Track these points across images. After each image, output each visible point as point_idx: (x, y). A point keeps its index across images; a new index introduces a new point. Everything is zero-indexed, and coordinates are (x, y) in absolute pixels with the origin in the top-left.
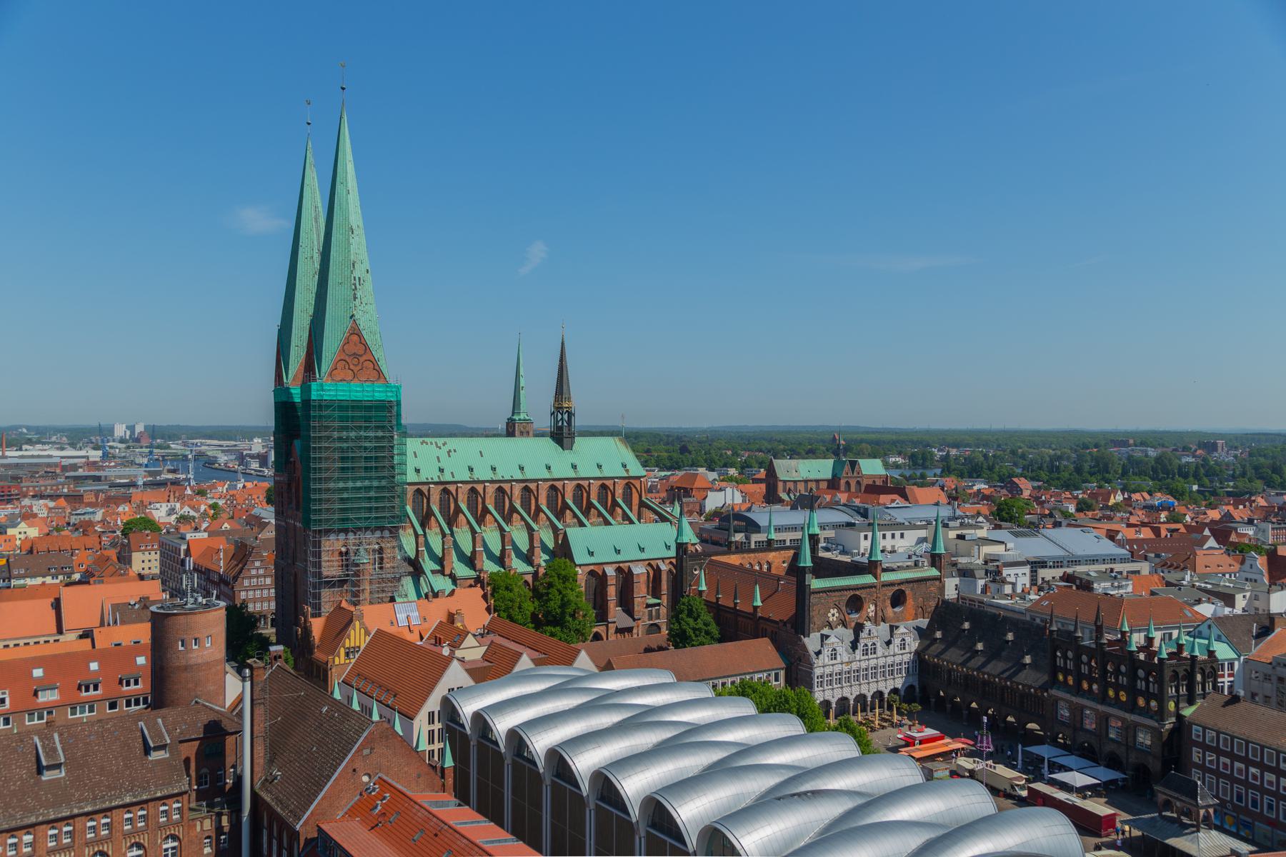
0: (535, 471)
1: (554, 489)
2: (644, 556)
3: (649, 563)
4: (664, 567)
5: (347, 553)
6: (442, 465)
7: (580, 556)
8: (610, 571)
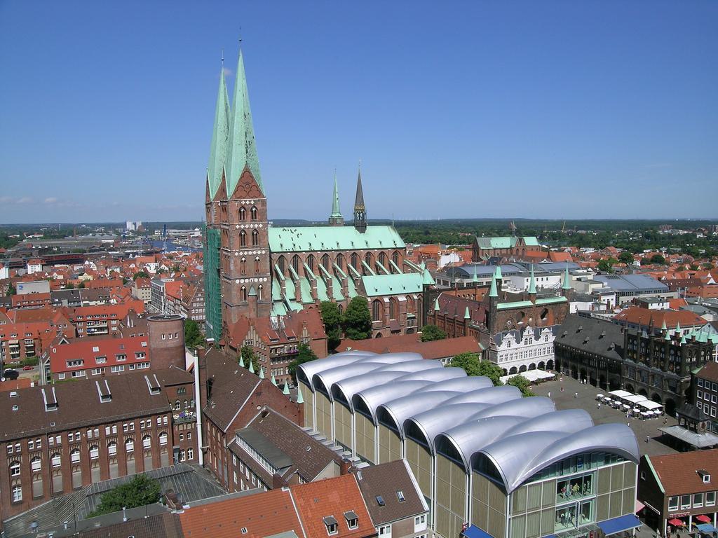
0: (345, 245)
1: (354, 254)
3: (408, 295)
4: (416, 297)
5: (245, 289)
7: (370, 292)
8: (386, 300)
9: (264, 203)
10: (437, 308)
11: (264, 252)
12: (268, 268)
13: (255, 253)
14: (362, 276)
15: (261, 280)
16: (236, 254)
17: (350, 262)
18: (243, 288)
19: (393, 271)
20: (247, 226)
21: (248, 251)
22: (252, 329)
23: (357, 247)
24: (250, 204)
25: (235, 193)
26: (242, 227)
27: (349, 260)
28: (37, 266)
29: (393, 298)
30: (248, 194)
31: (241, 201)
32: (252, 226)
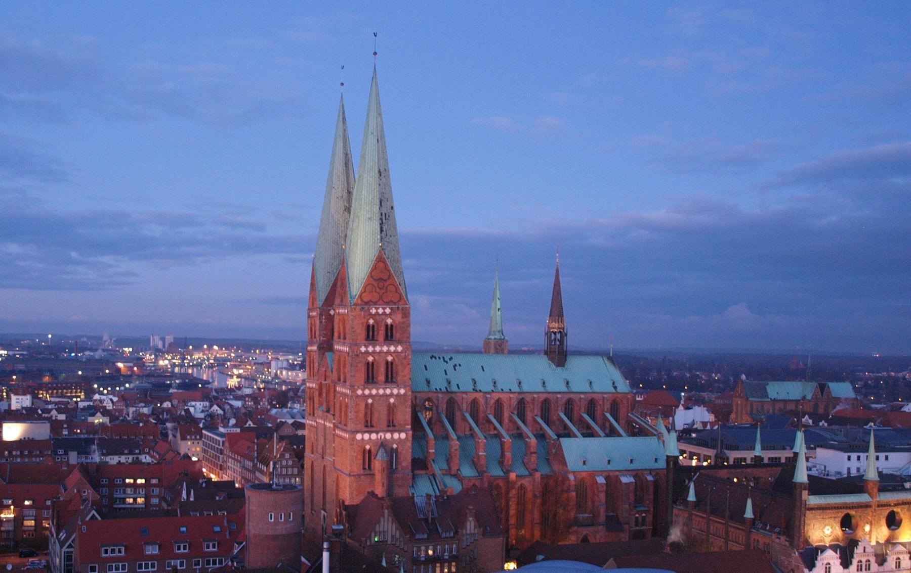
0: (532, 386)
2: (632, 467)
4: (650, 478)
5: (370, 451)
6: (448, 377)
9: (406, 314)
10: (692, 497)
11: (402, 391)
12: (408, 417)
13: (388, 391)
14: (559, 436)
15: (396, 436)
16: (359, 392)
17: (539, 414)
18: (368, 447)
19: (612, 433)
20: (378, 349)
21: (377, 389)
22: (386, 516)
23: (550, 389)
24: (384, 313)
25: (360, 296)
26: (370, 349)
27: (537, 411)
28: (24, 397)
29: (612, 480)
30: (381, 298)
31: (369, 310)
32: (385, 349)
